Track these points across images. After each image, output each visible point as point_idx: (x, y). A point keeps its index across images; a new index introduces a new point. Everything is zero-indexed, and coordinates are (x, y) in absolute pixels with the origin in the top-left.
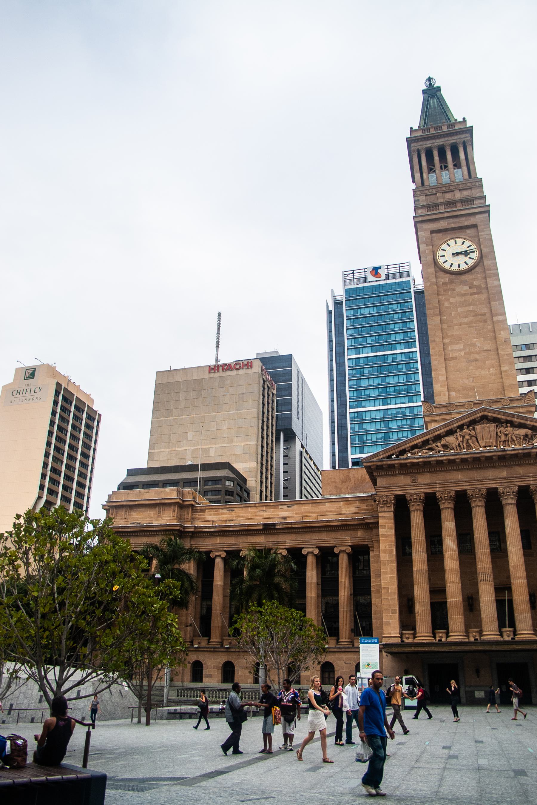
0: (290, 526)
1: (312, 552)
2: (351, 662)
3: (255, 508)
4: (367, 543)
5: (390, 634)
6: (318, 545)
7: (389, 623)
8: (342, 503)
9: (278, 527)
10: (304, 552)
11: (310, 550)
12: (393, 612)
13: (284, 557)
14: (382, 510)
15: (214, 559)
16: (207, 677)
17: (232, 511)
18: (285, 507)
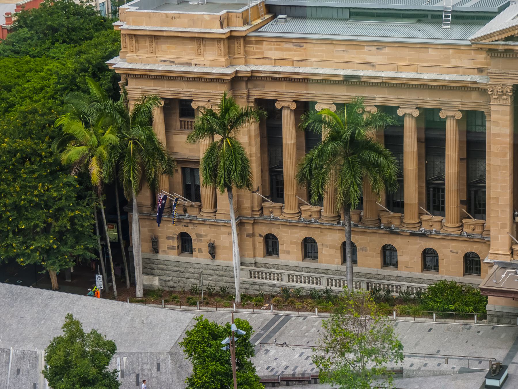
0: (380, 81)
1: (411, 115)
2: (459, 251)
3: (332, 46)
4: (482, 110)
5: (498, 250)
6: (419, 106)
7: (497, 238)
8: (451, 51)
9: (363, 80)
10: (400, 112)
11: (408, 111)
12: (503, 226)
13: (373, 116)
14: (496, 102)
15: (281, 110)
16: (284, 253)
17: (301, 47)
18: (373, 49)
